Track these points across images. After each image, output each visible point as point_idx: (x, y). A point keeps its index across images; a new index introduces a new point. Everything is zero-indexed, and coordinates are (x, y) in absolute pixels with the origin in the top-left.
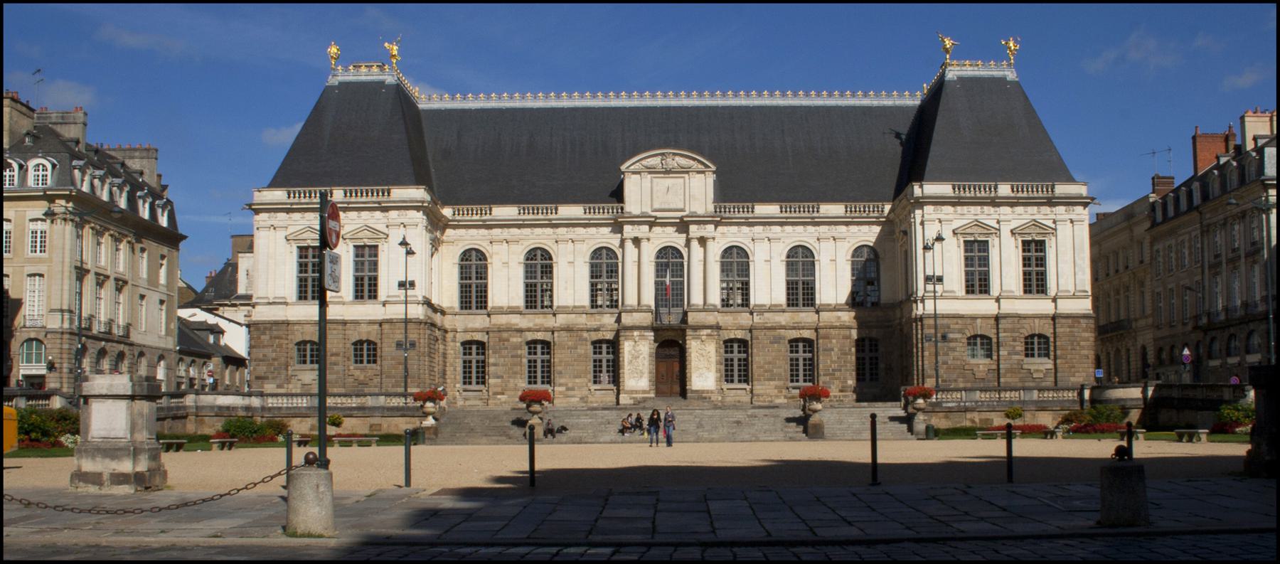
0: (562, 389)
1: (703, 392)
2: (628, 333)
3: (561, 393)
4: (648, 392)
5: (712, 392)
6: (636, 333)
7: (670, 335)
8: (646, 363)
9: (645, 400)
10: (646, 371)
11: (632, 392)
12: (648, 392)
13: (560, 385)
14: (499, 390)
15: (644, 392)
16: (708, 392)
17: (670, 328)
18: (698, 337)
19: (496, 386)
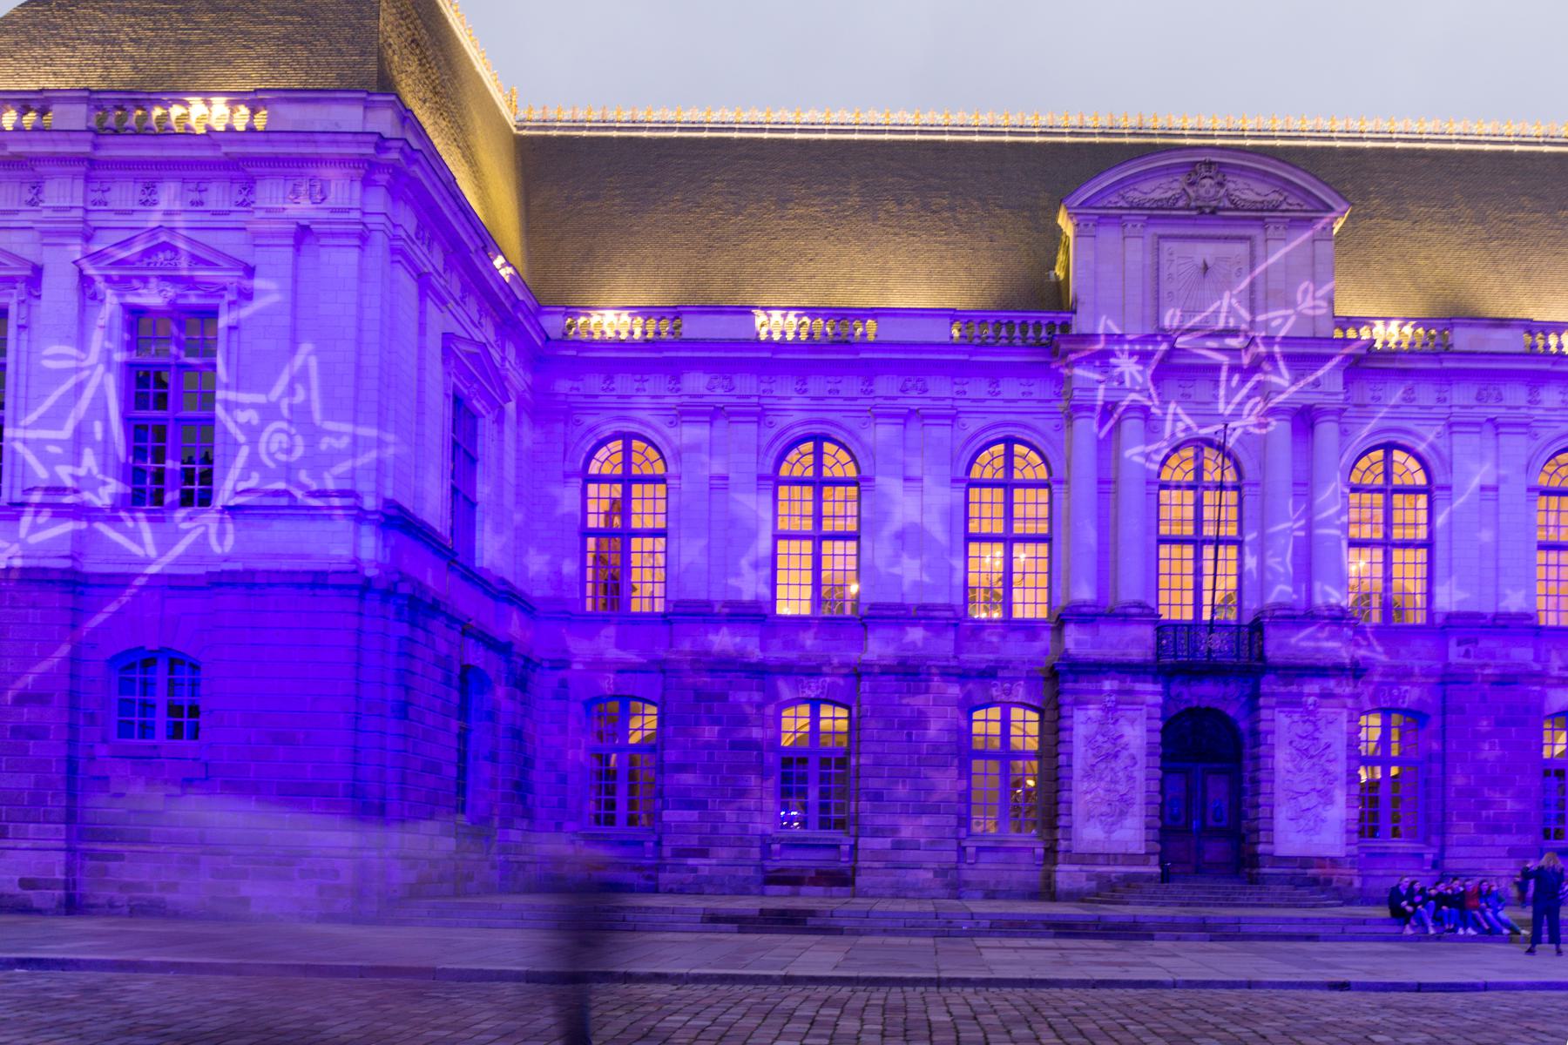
0: (887, 843)
1: (1306, 862)
2: (1084, 685)
3: (876, 854)
4: (1143, 859)
5: (1334, 861)
6: (1107, 685)
7: (1206, 693)
8: (1140, 774)
9: (1128, 880)
10: (1139, 797)
11: (1090, 858)
12: (1143, 859)
13: (877, 832)
14: (694, 841)
15: (1130, 858)
16: (1321, 861)
17: (1211, 670)
18: (1292, 703)
19: (683, 828)
